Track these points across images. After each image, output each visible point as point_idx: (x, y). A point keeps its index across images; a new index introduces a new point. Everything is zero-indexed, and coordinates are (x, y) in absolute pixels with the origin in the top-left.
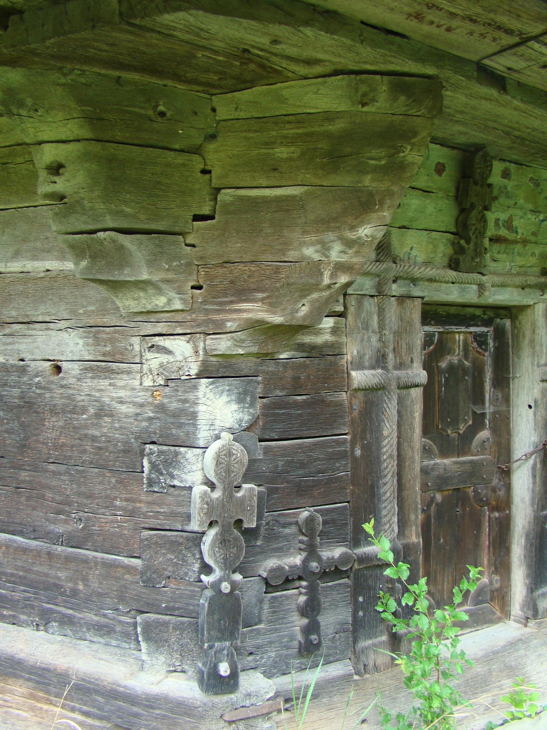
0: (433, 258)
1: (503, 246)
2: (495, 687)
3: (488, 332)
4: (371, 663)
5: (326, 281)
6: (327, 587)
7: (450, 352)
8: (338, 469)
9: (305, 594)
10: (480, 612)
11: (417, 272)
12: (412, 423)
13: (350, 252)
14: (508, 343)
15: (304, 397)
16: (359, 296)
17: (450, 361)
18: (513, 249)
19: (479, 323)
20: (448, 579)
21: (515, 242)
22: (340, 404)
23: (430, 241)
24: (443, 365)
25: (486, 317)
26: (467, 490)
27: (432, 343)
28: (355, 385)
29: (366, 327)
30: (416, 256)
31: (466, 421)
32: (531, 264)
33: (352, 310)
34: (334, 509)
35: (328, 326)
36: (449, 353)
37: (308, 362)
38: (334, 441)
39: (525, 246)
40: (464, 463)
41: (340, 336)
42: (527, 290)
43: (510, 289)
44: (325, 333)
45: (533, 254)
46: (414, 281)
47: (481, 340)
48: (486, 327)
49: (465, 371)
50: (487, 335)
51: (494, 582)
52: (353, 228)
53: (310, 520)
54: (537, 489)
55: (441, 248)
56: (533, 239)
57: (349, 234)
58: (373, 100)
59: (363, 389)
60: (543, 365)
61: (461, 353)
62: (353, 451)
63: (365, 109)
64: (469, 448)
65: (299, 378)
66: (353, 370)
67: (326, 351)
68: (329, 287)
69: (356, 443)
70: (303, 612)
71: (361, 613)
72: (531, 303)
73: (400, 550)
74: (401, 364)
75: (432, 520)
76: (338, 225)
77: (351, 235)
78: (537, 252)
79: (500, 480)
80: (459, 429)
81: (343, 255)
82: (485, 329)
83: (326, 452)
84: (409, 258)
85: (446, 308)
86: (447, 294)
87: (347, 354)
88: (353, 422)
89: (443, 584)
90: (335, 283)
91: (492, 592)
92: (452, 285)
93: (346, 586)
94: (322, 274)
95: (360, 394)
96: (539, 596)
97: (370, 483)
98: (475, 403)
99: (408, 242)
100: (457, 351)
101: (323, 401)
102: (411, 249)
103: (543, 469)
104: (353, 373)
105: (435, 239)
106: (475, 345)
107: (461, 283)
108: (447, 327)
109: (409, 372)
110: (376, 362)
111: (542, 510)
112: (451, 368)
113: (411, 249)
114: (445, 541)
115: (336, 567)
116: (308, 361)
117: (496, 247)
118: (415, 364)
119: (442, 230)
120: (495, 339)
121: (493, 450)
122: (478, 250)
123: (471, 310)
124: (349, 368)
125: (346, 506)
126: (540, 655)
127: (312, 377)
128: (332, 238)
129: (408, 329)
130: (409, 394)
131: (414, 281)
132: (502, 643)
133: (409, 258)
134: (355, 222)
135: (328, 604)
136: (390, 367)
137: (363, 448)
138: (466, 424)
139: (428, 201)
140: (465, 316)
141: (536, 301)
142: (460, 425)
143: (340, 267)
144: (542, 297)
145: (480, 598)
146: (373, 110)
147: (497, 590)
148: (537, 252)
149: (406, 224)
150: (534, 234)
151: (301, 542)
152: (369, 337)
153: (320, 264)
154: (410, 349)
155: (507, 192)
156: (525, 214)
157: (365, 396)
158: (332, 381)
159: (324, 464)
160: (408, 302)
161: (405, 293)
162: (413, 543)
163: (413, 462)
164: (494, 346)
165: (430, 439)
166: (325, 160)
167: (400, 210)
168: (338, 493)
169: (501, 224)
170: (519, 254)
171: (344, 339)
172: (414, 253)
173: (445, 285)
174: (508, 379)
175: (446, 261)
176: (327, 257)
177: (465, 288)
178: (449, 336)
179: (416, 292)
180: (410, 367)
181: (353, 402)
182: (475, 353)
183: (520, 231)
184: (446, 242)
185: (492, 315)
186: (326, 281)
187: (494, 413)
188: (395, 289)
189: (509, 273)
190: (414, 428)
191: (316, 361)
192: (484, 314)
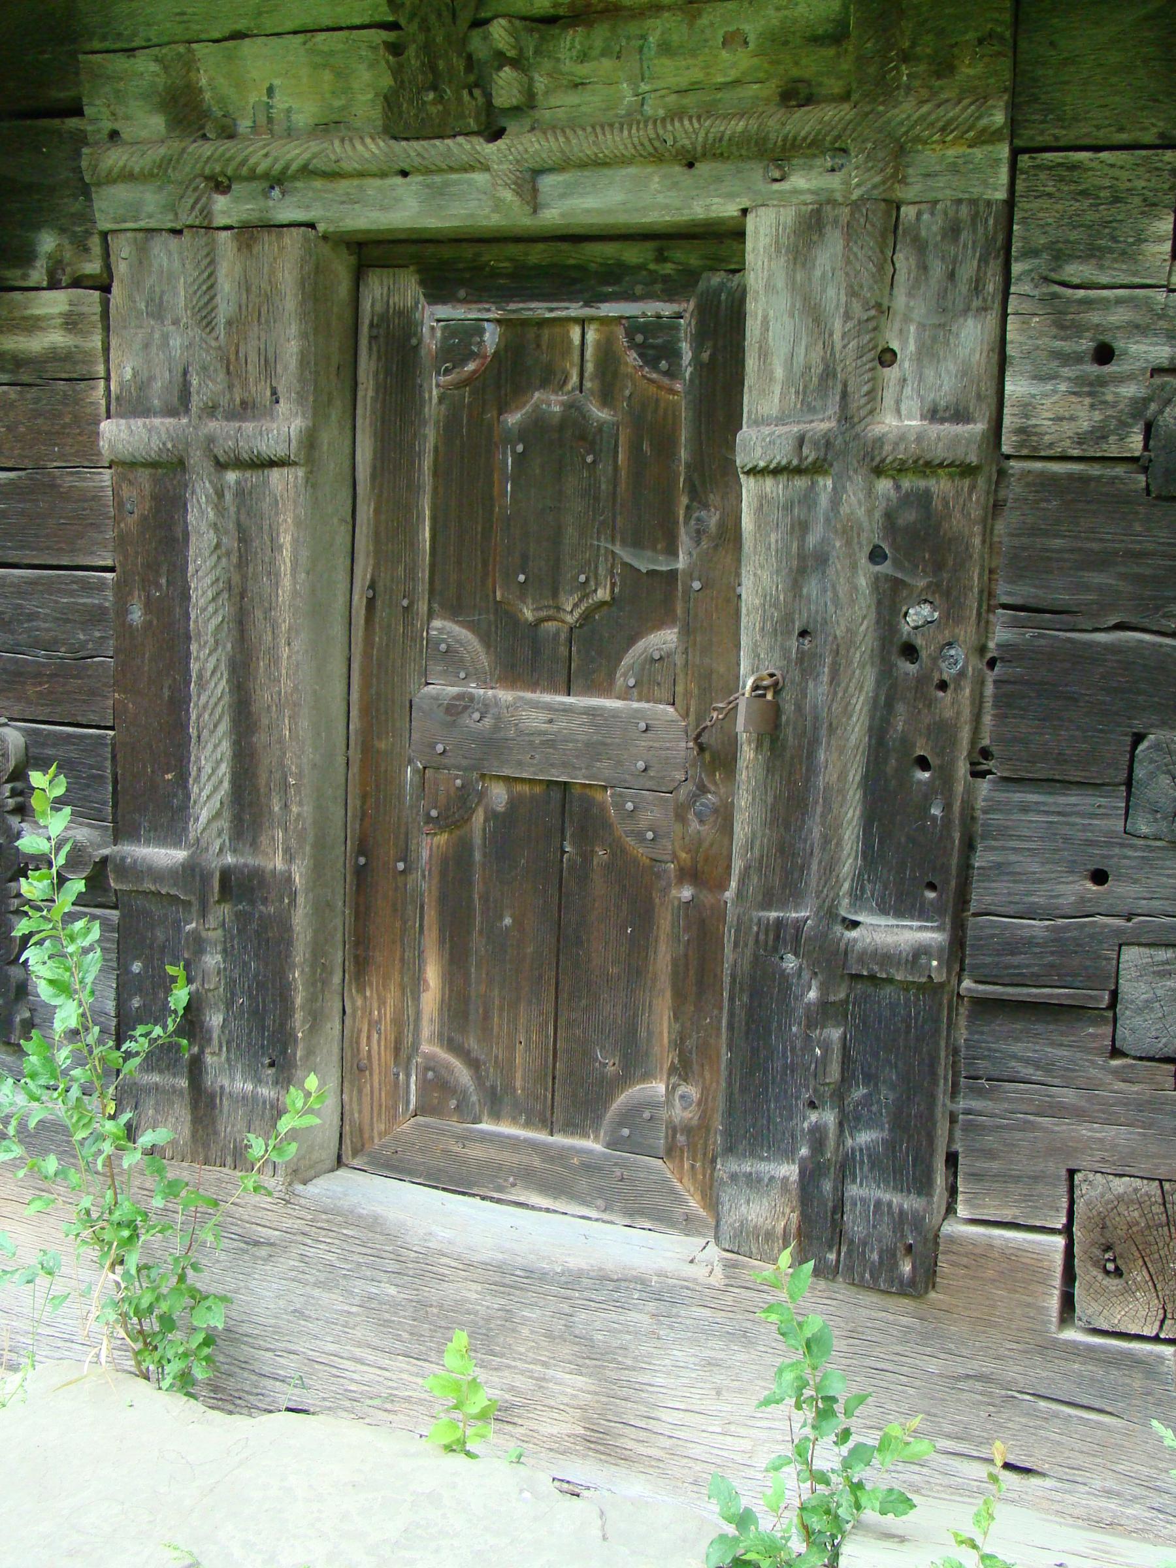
0: (343, 108)
2: (522, 1372)
7: (550, 378)
10: (618, 1172)
11: (264, 154)
15: (12, 475)
16: (140, 235)
17: (537, 406)
18: (643, 37)
20: (529, 1039)
23: (318, 60)
24: (513, 419)
25: (668, 268)
26: (598, 796)
29: (157, 310)
30: (289, 111)
31: (585, 590)
32: (733, 74)
33: (121, 268)
35: (55, 310)
36: (544, 384)
37: (13, 396)
39: (698, 14)
40: (567, 710)
41: (85, 334)
42: (702, 168)
43: (632, 170)
44: (49, 326)
45: (733, 40)
46: (277, 181)
47: (654, 344)
48: (670, 301)
50: (677, 328)
61: (588, 384)
62: (122, 611)
67: (52, 369)
69: (130, 593)
72: (731, 210)
74: (244, 403)
75: (478, 856)
78: (751, 29)
80: (559, 609)
82: (666, 309)
83: (57, 602)
84: (270, 120)
85: (513, 250)
86: (383, 208)
89: (511, 1049)
91: (673, 1129)
92: (399, 180)
96: (734, 1177)
97: (166, 693)
98: (637, 542)
99: (254, 74)
100: (574, 379)
101: (53, 486)
102: (270, 91)
103: (769, 770)
105: (332, 53)
106: (632, 358)
108: (512, 306)
109: (249, 427)
111: (767, 904)
113: (270, 91)
114: (518, 922)
118: (283, 407)
119: (357, 21)
120: (700, 339)
122: (441, 64)
123: (609, 250)
125: (104, 737)
126: (711, 1363)
129: (264, 309)
130: (266, 483)
131: (277, 181)
132: (576, 1262)
133: (270, 120)
137: (148, 606)
138: (585, 596)
140: (581, 268)
141: (745, 203)
142: (562, 598)
144: (776, 186)
145: (626, 1132)
147: (688, 1130)
148: (751, 29)
149: (241, 25)
152: (165, 337)
154: (268, 365)
157: (156, 481)
158: (70, 441)
159: (48, 630)
160: (267, 244)
161: (254, 217)
164: (696, 358)
165: (471, 626)
168: (84, 701)
170: (665, 49)
172: (281, 102)
173: (378, 182)
177: (446, 184)
178: (546, 333)
180: (270, 413)
184: (371, 56)
185: (694, 261)
188: (224, 209)
190: (277, 575)
191: (32, 393)
192: (661, 258)
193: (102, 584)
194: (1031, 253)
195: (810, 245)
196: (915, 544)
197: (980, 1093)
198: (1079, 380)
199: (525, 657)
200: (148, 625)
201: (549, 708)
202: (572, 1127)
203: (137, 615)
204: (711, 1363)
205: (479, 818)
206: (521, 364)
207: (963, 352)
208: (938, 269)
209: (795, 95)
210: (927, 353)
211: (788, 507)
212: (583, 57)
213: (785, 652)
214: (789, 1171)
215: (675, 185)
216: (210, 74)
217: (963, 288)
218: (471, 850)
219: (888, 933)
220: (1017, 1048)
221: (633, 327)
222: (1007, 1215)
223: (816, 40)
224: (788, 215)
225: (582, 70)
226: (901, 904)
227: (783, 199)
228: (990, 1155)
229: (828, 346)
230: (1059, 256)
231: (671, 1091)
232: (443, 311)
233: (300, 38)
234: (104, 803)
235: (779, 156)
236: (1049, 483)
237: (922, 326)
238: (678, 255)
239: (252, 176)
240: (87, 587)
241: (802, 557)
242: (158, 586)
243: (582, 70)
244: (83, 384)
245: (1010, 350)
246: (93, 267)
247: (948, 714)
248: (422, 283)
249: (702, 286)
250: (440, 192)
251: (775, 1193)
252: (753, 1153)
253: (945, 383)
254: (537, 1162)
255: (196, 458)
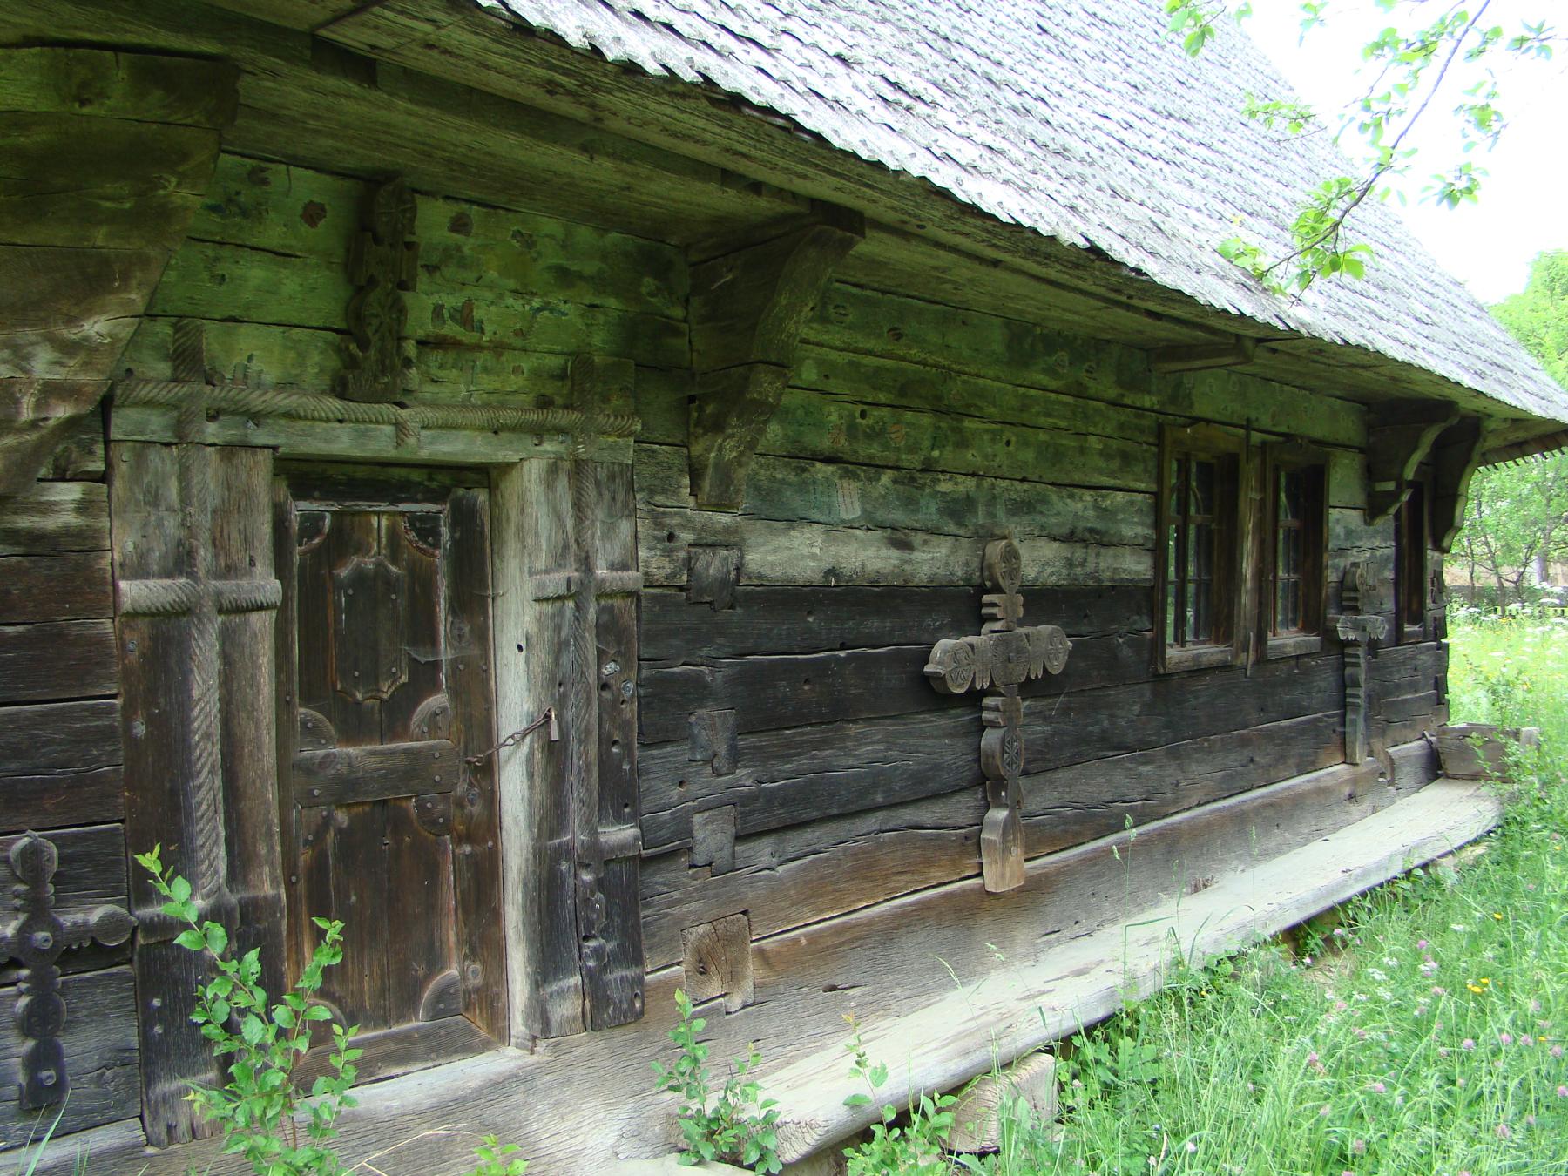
1: (451, 356)
2: (462, 1163)
3: (440, 512)
4: (183, 1126)
5: (27, 413)
6: (81, 980)
7: (362, 549)
8: (96, 759)
9: (27, 992)
10: (442, 1032)
11: (256, 401)
12: (253, 677)
13: (72, 363)
14: (482, 533)
15: (20, 628)
17: (358, 565)
19: (419, 496)
20: (372, 972)
21: (478, 347)
22: (99, 642)
24: (344, 573)
25: (434, 485)
26: (404, 804)
27: (318, 532)
28: (126, 604)
29: (154, 499)
30: (261, 372)
31: (395, 677)
32: (515, 388)
33: (122, 468)
34: (90, 833)
36: (357, 551)
37: (27, 564)
38: (87, 708)
39: (501, 355)
40: (393, 752)
41: (96, 516)
42: (504, 435)
45: (517, 370)
46: (257, 417)
47: (425, 528)
49: (390, 584)
51: (470, 975)
52: (71, 321)
53: (32, 854)
54: (538, 798)
55: (315, 357)
56: (517, 342)
57: (65, 332)
58: (102, 95)
59: (144, 614)
60: (540, 572)
62: (128, 728)
63: (86, 110)
64: (406, 727)
65: (8, 593)
66: (125, 578)
68: (34, 425)
69: (135, 713)
70: (30, 1024)
71: (158, 1029)
72: (516, 459)
73: (233, 909)
74: (228, 568)
76: (42, 314)
77: (71, 334)
79: (471, 785)
80: (379, 690)
81: (58, 368)
82: (433, 508)
84: (246, 376)
85: (348, 469)
86: (326, 441)
87: (111, 550)
88: (127, 674)
89: (361, 982)
90: (46, 419)
91: (467, 993)
92: (338, 425)
93: (124, 977)
94: (17, 402)
95: (142, 623)
96: (551, 995)
97: (168, 785)
98: (415, 642)
102: (250, 358)
103: (548, 762)
104: (123, 584)
107: (357, 421)
109: (244, 583)
110: (176, 564)
111: (551, 838)
112: (360, 578)
113: (250, 358)
114: (360, 898)
115: (93, 939)
116: (26, 562)
117: (435, 357)
118: (258, 569)
120: (453, 526)
121: (454, 729)
122: (387, 362)
123: (403, 472)
124: (117, 574)
125: (116, 829)
126: (557, 1103)
127: (35, 591)
128: (33, 338)
129: (243, 504)
130: (246, 623)
131: (257, 417)
133: (246, 376)
134: (75, 311)
135: (85, 1012)
136: (201, 574)
137: (149, 722)
138: (395, 681)
139: (286, 272)
141: (524, 455)
143: (51, 391)
146: (102, 112)
147: (477, 990)
148: (525, 366)
149: (236, 313)
150: (519, 333)
151: (17, 895)
152: (160, 520)
153: (13, 384)
154: (247, 541)
155: (463, 258)
156: (501, 296)
160: (244, 457)
161: (235, 439)
162: (265, 898)
163: (260, 748)
164: (452, 537)
166: (16, 198)
167: (224, 288)
169: (447, 315)
170: (486, 370)
171: (105, 522)
172: (255, 366)
174: (484, 598)
175: (326, 380)
176: (25, 371)
178: (357, 519)
179: (261, 437)
180: (249, 573)
181: (127, 637)
182: (414, 551)
183: (488, 328)
185: (448, 481)
186: (27, 413)
187: (454, 663)
189: (465, 405)
190: (258, 686)
191: (46, 562)
192: (431, 479)
193: (112, 707)
194: (641, 490)
195: (554, 480)
196: (608, 629)
197: (648, 906)
198: (663, 550)
199: (354, 726)
200: (149, 734)
201: (381, 753)
202: (402, 1018)
203: (140, 729)
204: (557, 1103)
205: (330, 837)
206: (342, 541)
207: (623, 537)
208: (607, 495)
209: (544, 403)
210: (606, 536)
211: (554, 616)
212: (441, 367)
213: (552, 695)
214: (576, 980)
215: (489, 443)
216: (212, 338)
217: (619, 504)
218: (326, 856)
219: (619, 834)
220: (658, 878)
221: (413, 519)
222: (664, 962)
223: (553, 377)
224: (544, 464)
225: (441, 373)
226: (620, 819)
227: (541, 455)
228: (654, 935)
229: (565, 533)
230: (652, 492)
231: (463, 973)
232: (304, 505)
233: (282, 329)
234: (120, 881)
235: (539, 432)
236: (654, 598)
237: (603, 522)
238: (440, 477)
239: (244, 413)
240: (97, 713)
241: (560, 644)
242: (157, 706)
243: (441, 373)
244: (93, 555)
245: (640, 536)
246: (98, 466)
247: (629, 716)
248: (289, 486)
249: (452, 496)
250: (364, 434)
251: (571, 995)
252: (556, 979)
253: (616, 552)
254: (393, 1047)
255: (209, 606)
